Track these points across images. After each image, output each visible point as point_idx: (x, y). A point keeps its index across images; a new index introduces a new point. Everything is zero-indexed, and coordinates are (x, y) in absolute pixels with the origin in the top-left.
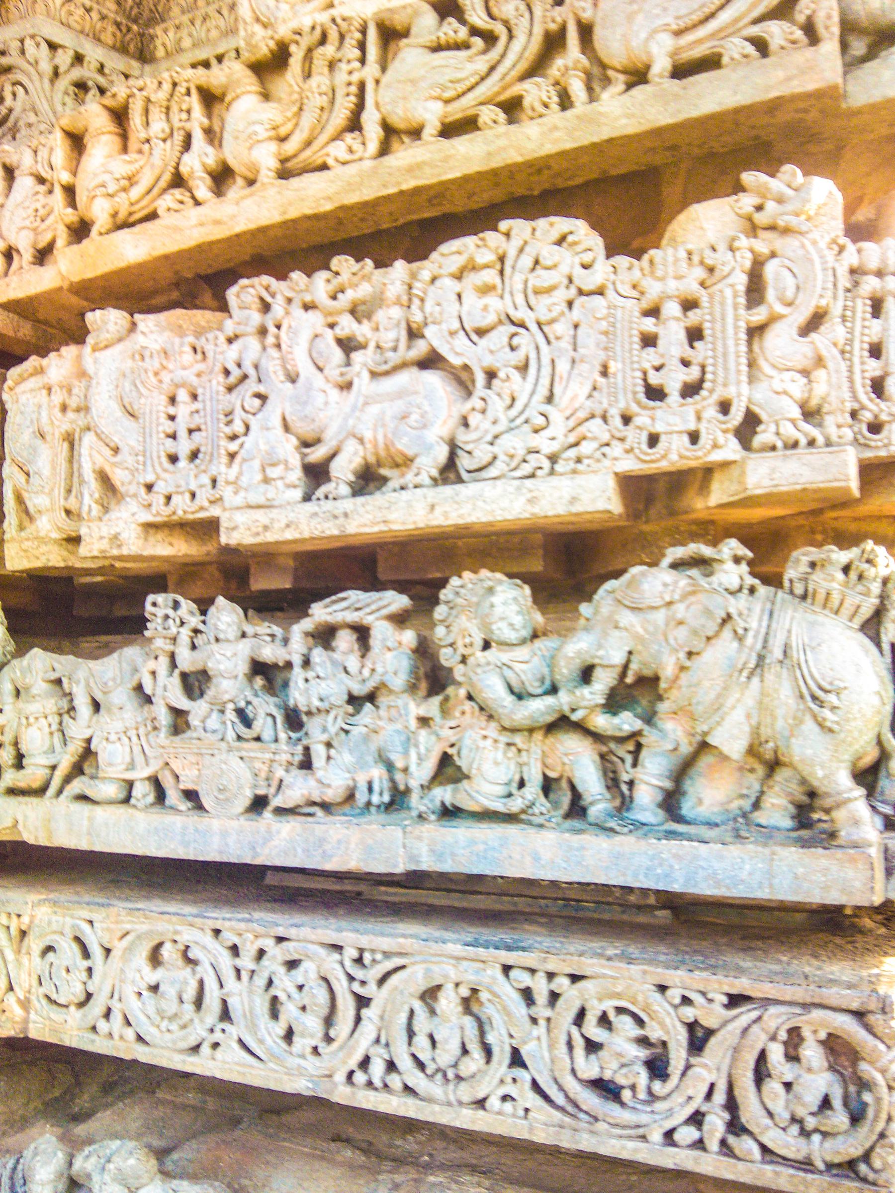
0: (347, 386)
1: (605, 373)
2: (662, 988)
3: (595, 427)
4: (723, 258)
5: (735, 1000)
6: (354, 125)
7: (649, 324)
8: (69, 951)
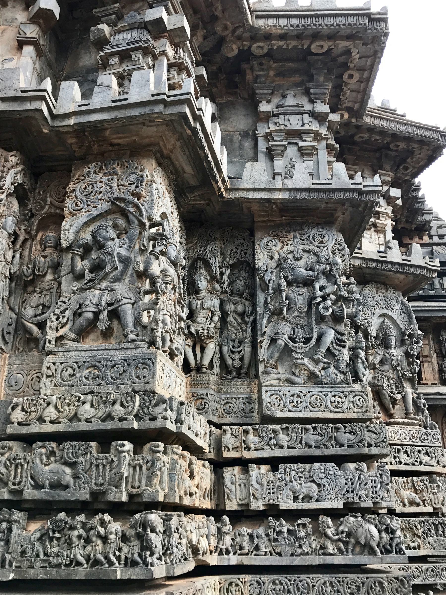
0: (301, 484)
1: (341, 487)
2: (358, 578)
3: (340, 495)
4: (355, 474)
5: (367, 578)
6: (300, 442)
7: (346, 481)
8: (256, 584)
